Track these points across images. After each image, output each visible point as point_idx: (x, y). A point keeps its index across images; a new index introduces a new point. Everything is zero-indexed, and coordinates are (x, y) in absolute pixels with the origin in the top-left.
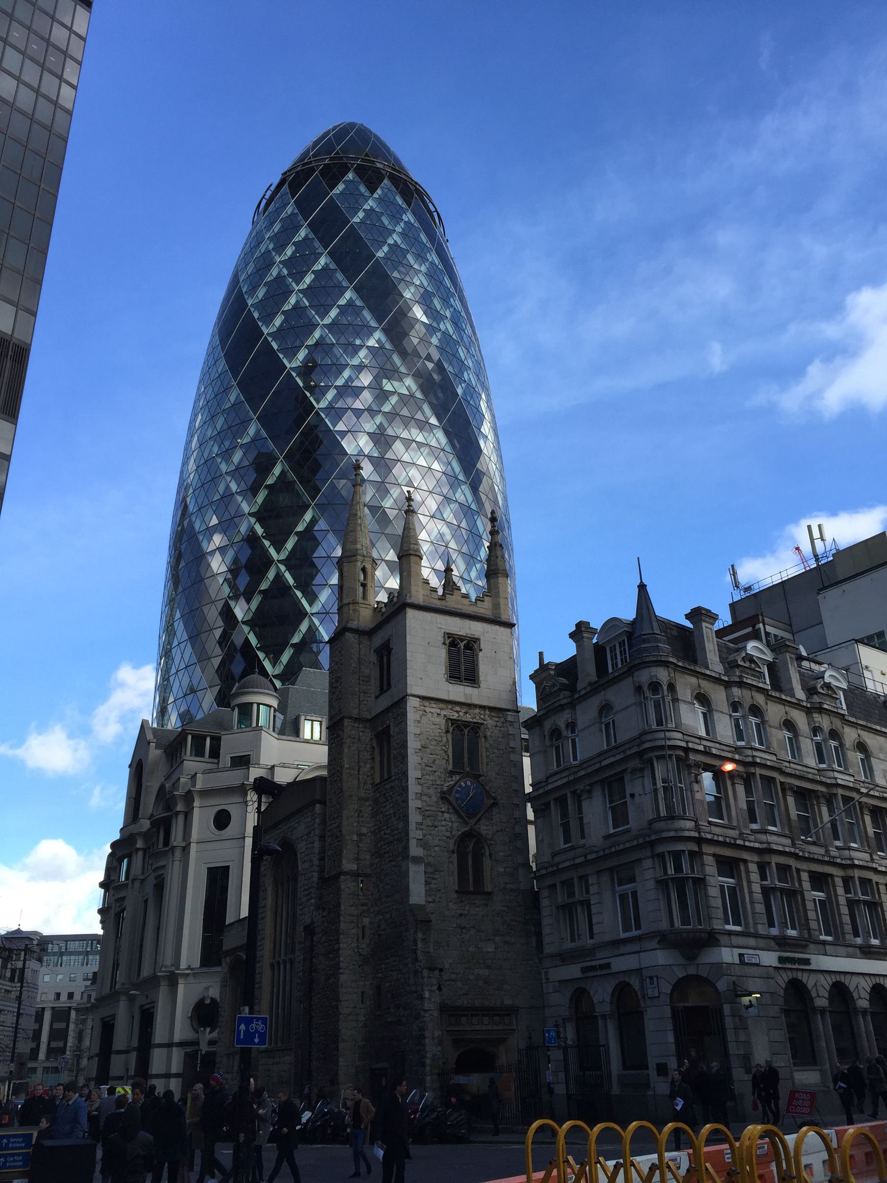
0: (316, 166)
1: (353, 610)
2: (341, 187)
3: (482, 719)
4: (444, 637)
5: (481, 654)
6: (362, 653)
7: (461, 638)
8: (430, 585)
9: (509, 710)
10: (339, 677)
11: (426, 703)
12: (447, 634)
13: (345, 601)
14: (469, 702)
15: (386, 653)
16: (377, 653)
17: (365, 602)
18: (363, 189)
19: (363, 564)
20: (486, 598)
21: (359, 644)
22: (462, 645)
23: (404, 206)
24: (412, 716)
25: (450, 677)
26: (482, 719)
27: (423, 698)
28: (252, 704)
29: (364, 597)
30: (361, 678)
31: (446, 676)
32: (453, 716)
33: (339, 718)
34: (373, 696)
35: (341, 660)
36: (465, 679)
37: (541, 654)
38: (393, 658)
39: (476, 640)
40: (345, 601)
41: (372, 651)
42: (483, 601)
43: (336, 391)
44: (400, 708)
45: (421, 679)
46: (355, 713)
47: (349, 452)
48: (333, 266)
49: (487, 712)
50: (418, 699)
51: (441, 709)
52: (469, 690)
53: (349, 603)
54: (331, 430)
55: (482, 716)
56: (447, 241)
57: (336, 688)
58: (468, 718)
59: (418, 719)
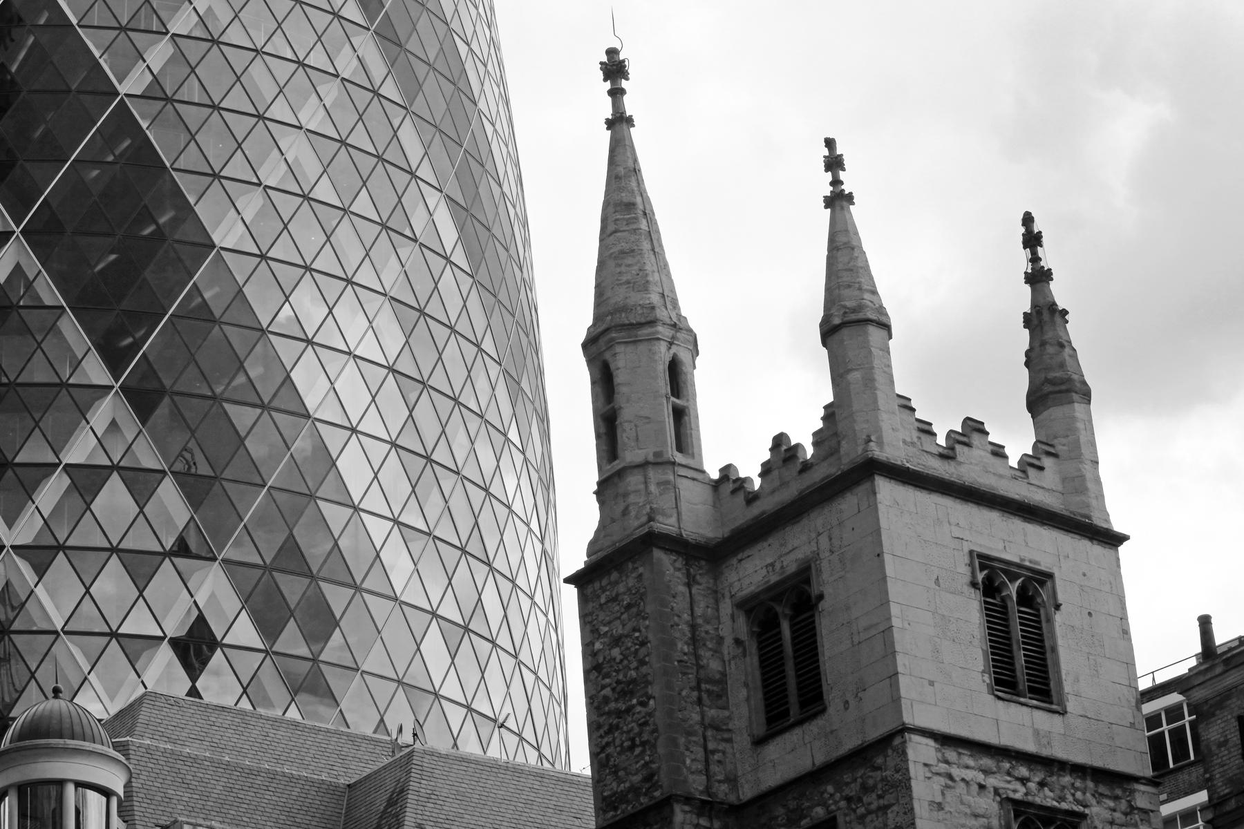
1: (659, 484)
3: (1078, 802)
4: (971, 564)
5: (1058, 618)
6: (699, 611)
7: (1011, 570)
9: (1136, 779)
10: (633, 681)
11: (951, 755)
12: (980, 556)
14: (1045, 752)
15: (788, 611)
16: (748, 613)
19: (674, 349)
20: (1047, 462)
21: (689, 585)
22: (1013, 589)
24: (923, 789)
25: (998, 682)
26: (1078, 802)
27: (945, 740)
28: (61, 783)
30: (703, 686)
31: (986, 677)
32: (1015, 791)
33: (644, 800)
34: (742, 741)
35: (635, 630)
36: (1031, 690)
37: (1205, 623)
38: (825, 626)
39: (1045, 578)
40: (630, 455)
41: (726, 608)
42: (1041, 468)
44: (879, 768)
45: (932, 683)
46: (697, 784)
47: (123, 89)
49: (1090, 784)
50: (931, 742)
51: (986, 772)
52: (1042, 720)
55: (1079, 795)
57: (619, 714)
58: (1047, 798)
59: (939, 799)
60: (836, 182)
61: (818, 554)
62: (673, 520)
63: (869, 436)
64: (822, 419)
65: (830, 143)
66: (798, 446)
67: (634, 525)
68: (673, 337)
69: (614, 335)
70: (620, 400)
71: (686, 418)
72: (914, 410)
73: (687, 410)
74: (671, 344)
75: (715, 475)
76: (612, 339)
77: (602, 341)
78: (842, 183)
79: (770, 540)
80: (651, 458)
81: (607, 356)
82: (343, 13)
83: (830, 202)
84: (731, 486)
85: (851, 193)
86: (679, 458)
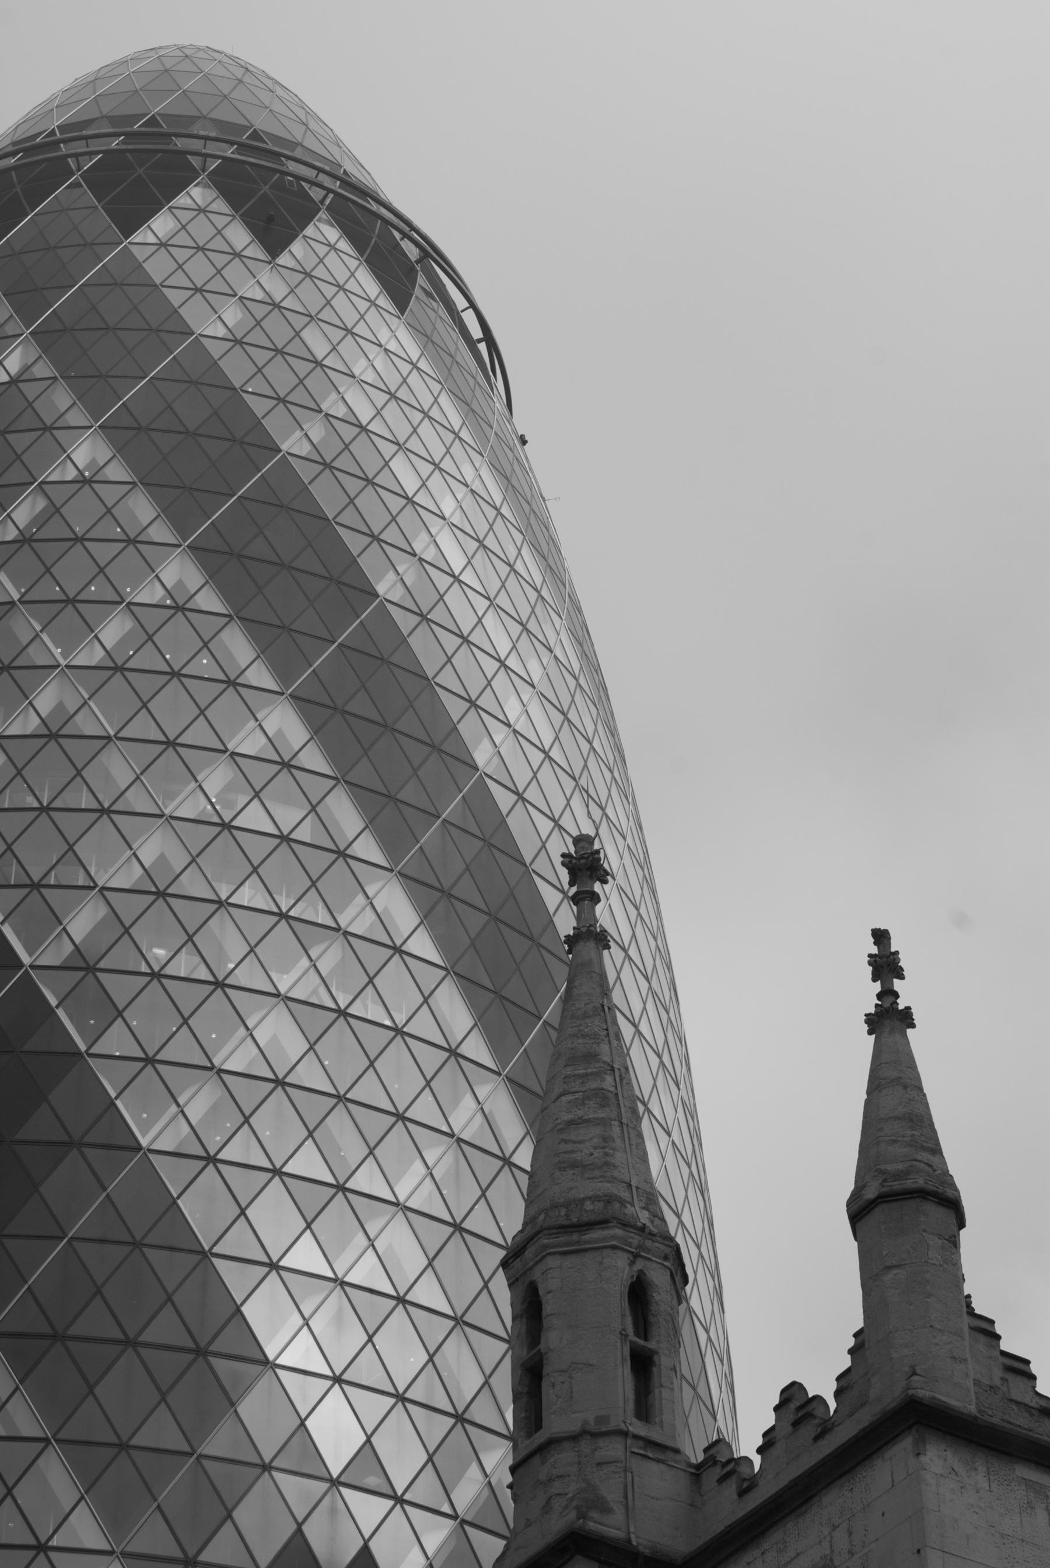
0: (76, 156)
2: (162, 224)
8: (1005, 1345)
13: (556, 1424)
17: (655, 1435)
18: (239, 236)
19: (640, 1265)
23: (384, 302)
29: (644, 1409)
43: (103, 911)
47: (144, 1142)
48: (117, 471)
53: (574, 1438)
54: (78, 1054)
56: (524, 442)
60: (888, 994)
61: (831, 1560)
62: (618, 1516)
63: (913, 1367)
64: (851, 1352)
65: (881, 936)
66: (817, 1398)
67: (556, 1525)
68: (640, 1247)
69: (546, 1241)
70: (553, 1338)
71: (655, 1370)
72: (998, 1337)
73: (656, 1358)
74: (636, 1256)
75: (697, 1456)
76: (545, 1247)
77: (529, 1253)
78: (896, 995)
79: (766, 1545)
80: (592, 1427)
81: (536, 1275)
82: (464, 1050)
83: (875, 1022)
84: (717, 1472)
85: (908, 1008)
86: (638, 1428)
